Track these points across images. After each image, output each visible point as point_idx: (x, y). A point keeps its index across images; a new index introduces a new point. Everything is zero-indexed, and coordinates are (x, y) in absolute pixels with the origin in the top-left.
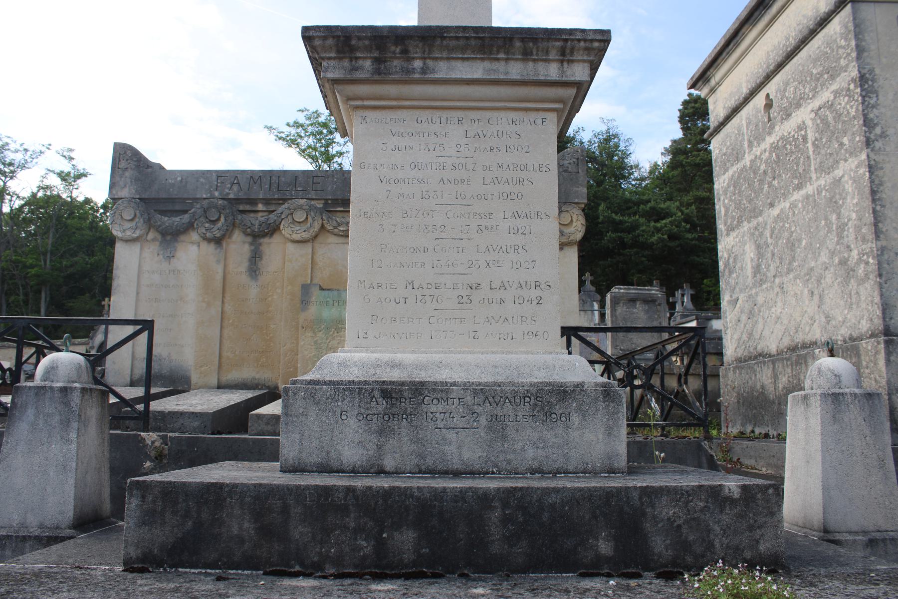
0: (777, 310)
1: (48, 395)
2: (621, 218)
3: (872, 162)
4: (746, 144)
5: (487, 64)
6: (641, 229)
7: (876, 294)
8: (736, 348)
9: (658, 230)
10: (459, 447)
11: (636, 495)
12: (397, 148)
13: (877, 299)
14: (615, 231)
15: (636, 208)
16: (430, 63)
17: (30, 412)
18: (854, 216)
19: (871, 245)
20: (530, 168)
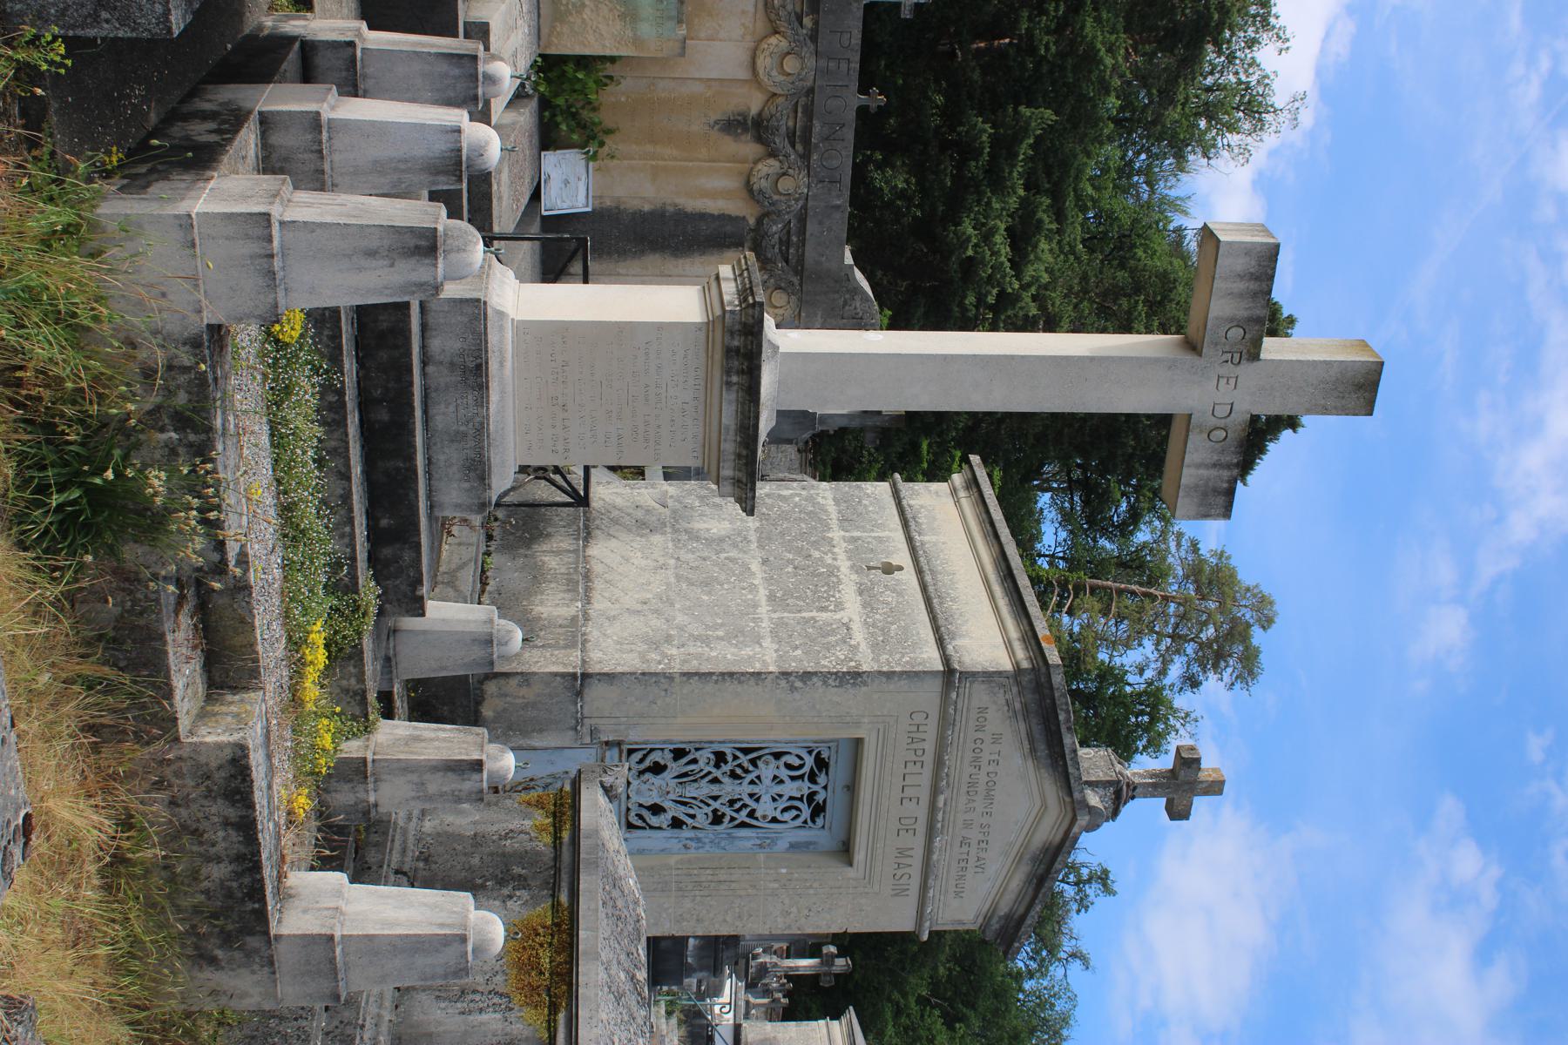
0: (638, 559)
1: (472, 85)
2: (1021, 157)
3: (763, 676)
4: (856, 534)
5: (733, 427)
6: (994, 200)
7: (626, 669)
8: (603, 500)
9: (987, 237)
10: (444, 414)
11: (416, 539)
12: (674, 353)
13: (620, 669)
14: (995, 141)
15: (1047, 186)
16: (735, 388)
17: (457, 72)
18: (714, 654)
19: (677, 667)
20: (658, 447)
